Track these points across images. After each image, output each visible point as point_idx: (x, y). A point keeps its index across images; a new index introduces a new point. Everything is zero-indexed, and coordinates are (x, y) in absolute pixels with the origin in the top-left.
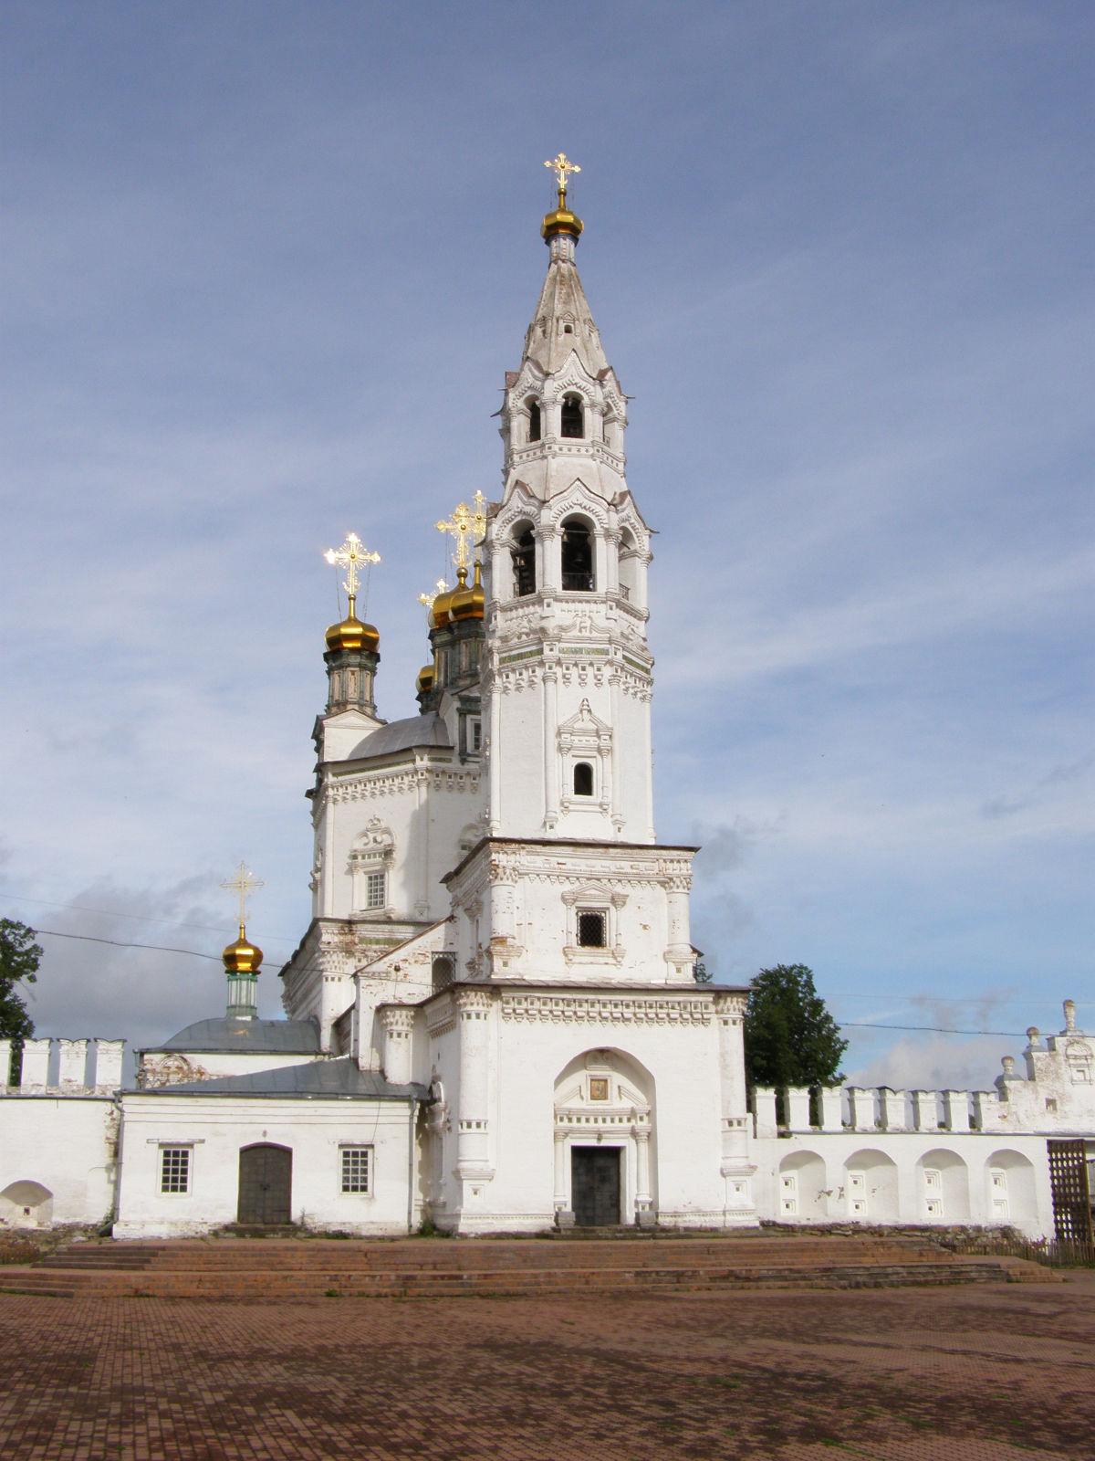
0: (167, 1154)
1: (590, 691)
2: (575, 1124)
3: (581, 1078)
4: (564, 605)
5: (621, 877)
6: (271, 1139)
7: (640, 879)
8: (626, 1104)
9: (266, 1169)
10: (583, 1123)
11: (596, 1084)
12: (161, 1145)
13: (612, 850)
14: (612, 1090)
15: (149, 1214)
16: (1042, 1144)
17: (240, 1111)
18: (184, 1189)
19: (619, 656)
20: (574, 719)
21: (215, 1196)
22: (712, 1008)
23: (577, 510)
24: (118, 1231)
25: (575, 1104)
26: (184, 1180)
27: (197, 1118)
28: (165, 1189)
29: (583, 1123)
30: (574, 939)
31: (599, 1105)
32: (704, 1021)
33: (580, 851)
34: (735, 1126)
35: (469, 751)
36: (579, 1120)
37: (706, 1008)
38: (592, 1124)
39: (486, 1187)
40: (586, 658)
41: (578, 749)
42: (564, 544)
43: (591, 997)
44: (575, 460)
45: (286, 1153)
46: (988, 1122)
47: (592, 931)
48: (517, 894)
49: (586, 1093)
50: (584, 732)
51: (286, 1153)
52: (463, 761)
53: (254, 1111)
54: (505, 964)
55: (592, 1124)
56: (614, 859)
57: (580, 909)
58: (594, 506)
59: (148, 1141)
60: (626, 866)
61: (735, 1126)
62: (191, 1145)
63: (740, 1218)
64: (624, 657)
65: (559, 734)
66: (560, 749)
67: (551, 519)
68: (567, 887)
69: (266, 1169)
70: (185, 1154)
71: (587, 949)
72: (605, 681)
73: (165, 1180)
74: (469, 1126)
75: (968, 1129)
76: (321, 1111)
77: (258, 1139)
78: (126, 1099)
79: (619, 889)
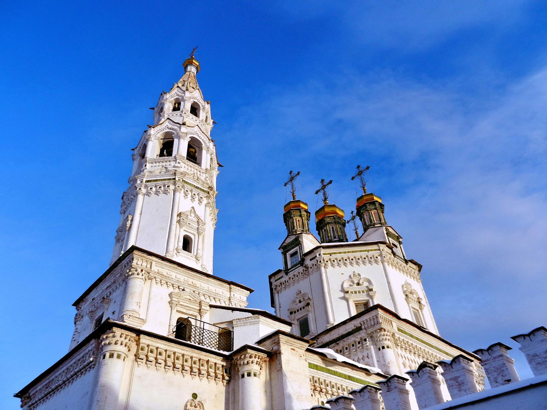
52: (287, 274)
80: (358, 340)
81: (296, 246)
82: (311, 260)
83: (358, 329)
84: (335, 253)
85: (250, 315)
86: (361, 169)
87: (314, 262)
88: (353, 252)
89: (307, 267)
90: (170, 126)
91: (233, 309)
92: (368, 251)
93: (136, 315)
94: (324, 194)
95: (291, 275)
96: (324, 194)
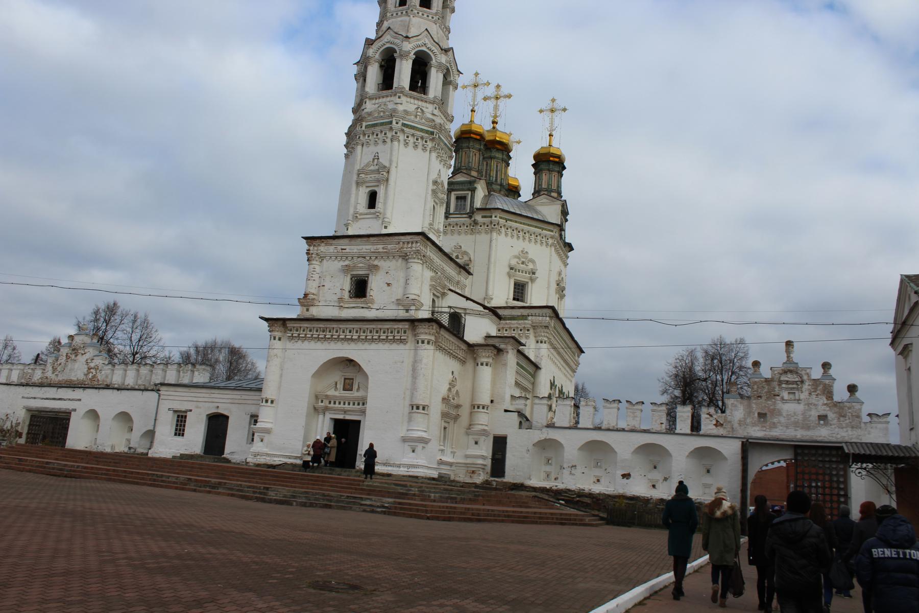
0: (178, 416)
1: (380, 148)
2: (332, 405)
3: (337, 377)
4: (374, 101)
5: (378, 255)
6: (221, 411)
7: (387, 255)
8: (360, 394)
9: (217, 426)
10: (337, 405)
11: (347, 381)
12: (175, 411)
13: (371, 239)
14: (355, 387)
15: (167, 446)
16: (736, 445)
17: (207, 395)
18: (183, 435)
19: (400, 124)
20: (368, 165)
21: (194, 441)
22: (409, 333)
23: (388, 45)
24: (150, 455)
25: (332, 392)
26: (184, 430)
27: (190, 399)
28: (176, 434)
29: (337, 405)
30: (346, 295)
31: (347, 394)
32: (402, 341)
33: (354, 241)
34: (415, 410)
35: (452, 211)
36: (335, 403)
37: (405, 332)
38: (342, 405)
39: (267, 438)
40: (378, 129)
41: (369, 182)
42: (381, 66)
43: (335, 325)
44: (400, 19)
45: (227, 418)
46: (707, 425)
47: (360, 288)
48: (318, 269)
49: (340, 386)
50: (373, 172)
51: (227, 418)
53: (213, 396)
54: (308, 310)
55: (342, 405)
56: (373, 244)
57: (353, 276)
58: (396, 41)
59: (169, 409)
60: (380, 248)
61: (415, 410)
62: (186, 412)
63: (426, 471)
64: (404, 125)
65: (358, 175)
66: (358, 184)
67: (375, 53)
68: (347, 263)
69: (217, 426)
70: (186, 417)
71: (354, 300)
72: (388, 140)
73: (176, 430)
74: (267, 401)
75: (689, 431)
76: (244, 397)
77: (215, 411)
78: (163, 388)
79: (376, 263)
80: (521, 327)
81: (469, 190)
82: (483, 217)
83: (524, 317)
84: (511, 221)
85: (481, 309)
86: (555, 105)
87: (487, 220)
88: (528, 225)
89: (476, 223)
90: (429, 46)
91: (468, 299)
92: (543, 229)
93: (524, 363)
94: (496, 108)
95: (450, 220)
96: (496, 108)
